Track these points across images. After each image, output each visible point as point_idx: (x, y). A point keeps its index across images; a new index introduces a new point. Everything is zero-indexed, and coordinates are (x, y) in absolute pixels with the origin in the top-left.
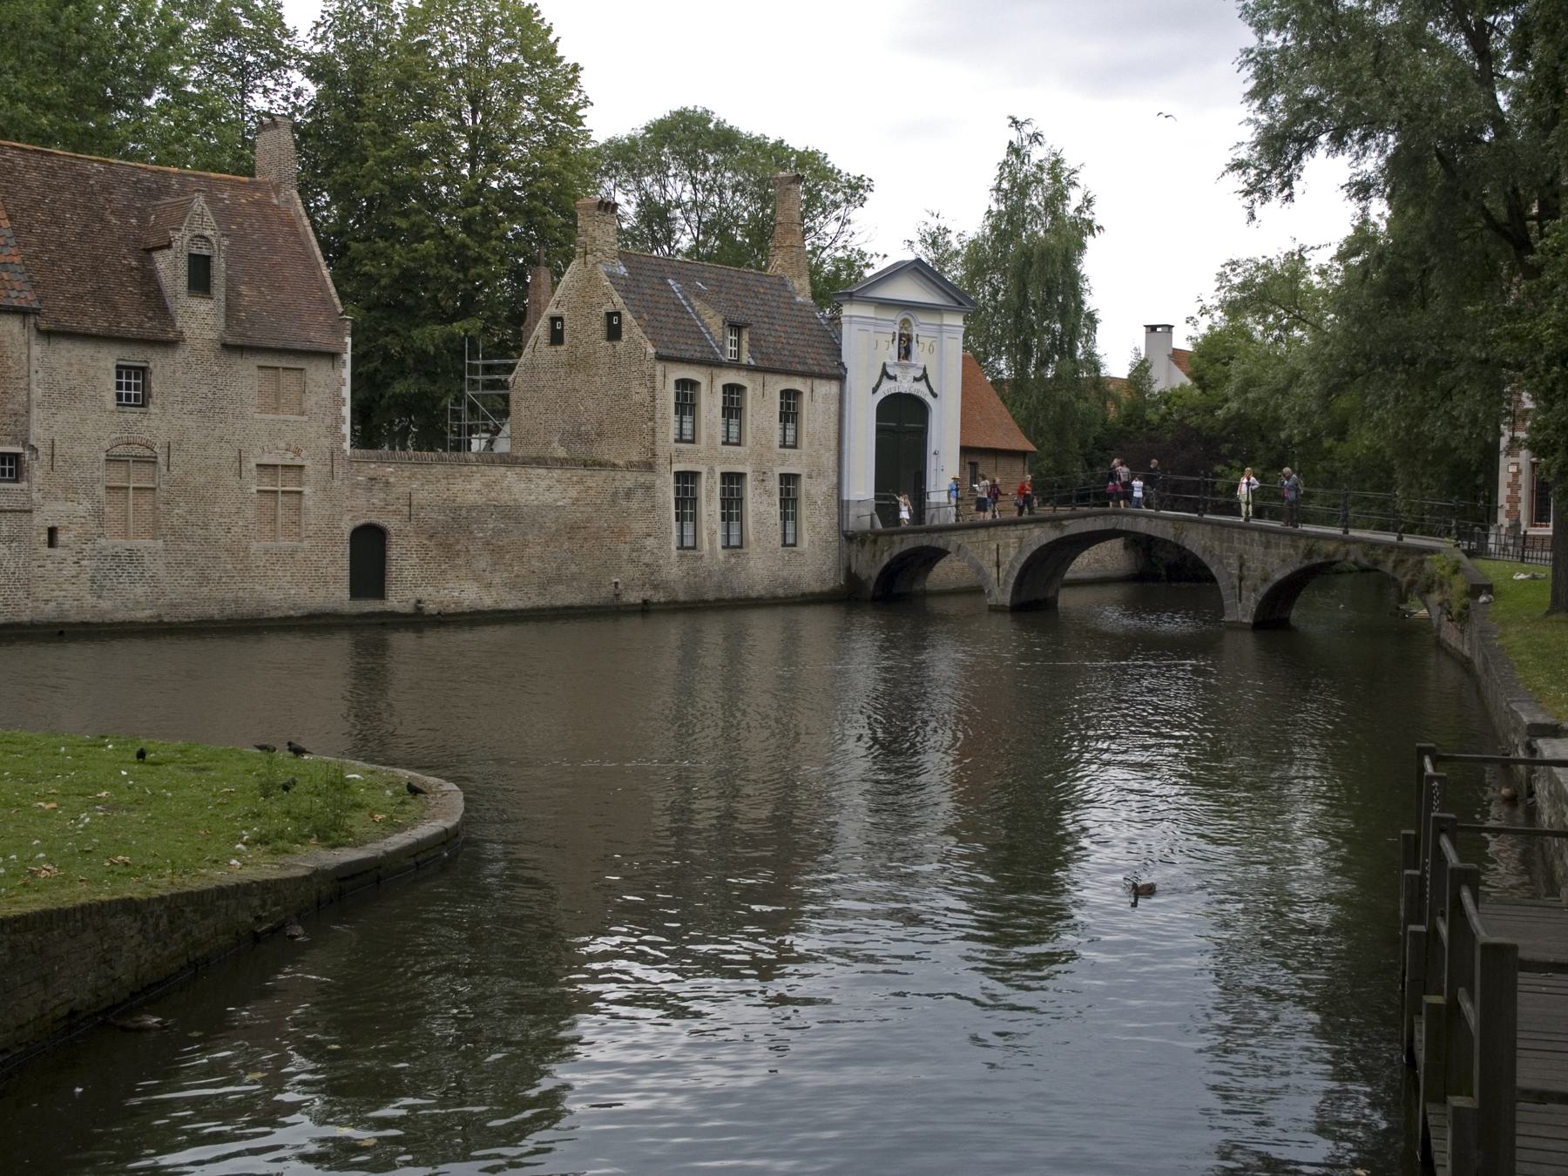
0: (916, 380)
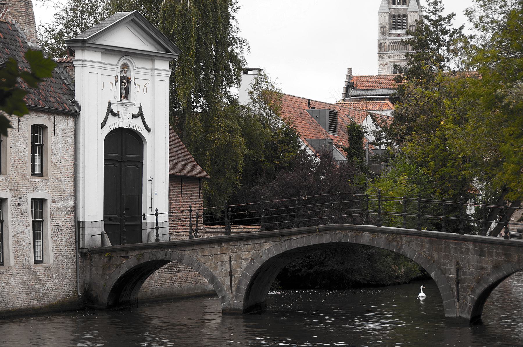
0: (134, 116)
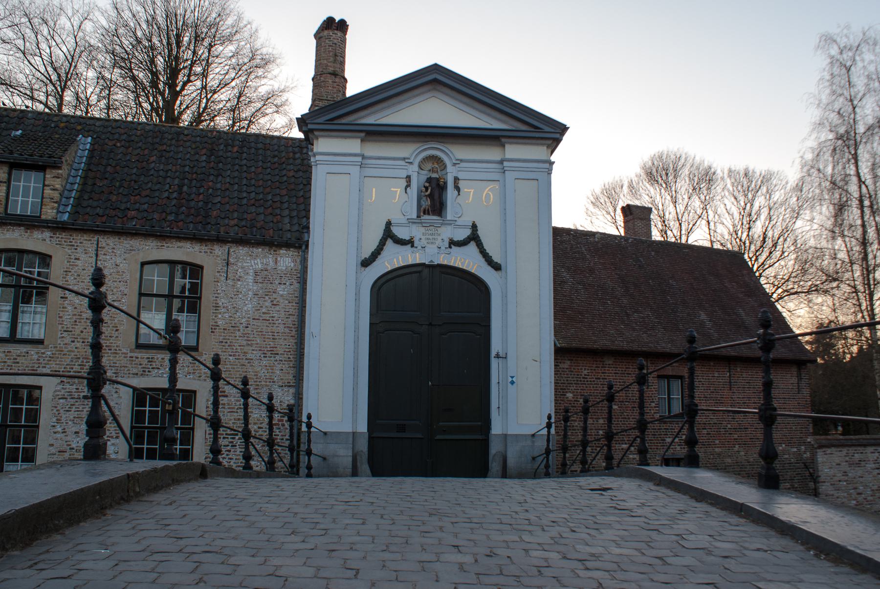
0: (453, 243)
